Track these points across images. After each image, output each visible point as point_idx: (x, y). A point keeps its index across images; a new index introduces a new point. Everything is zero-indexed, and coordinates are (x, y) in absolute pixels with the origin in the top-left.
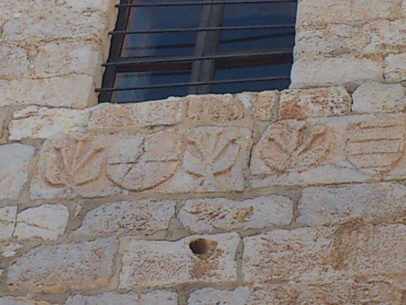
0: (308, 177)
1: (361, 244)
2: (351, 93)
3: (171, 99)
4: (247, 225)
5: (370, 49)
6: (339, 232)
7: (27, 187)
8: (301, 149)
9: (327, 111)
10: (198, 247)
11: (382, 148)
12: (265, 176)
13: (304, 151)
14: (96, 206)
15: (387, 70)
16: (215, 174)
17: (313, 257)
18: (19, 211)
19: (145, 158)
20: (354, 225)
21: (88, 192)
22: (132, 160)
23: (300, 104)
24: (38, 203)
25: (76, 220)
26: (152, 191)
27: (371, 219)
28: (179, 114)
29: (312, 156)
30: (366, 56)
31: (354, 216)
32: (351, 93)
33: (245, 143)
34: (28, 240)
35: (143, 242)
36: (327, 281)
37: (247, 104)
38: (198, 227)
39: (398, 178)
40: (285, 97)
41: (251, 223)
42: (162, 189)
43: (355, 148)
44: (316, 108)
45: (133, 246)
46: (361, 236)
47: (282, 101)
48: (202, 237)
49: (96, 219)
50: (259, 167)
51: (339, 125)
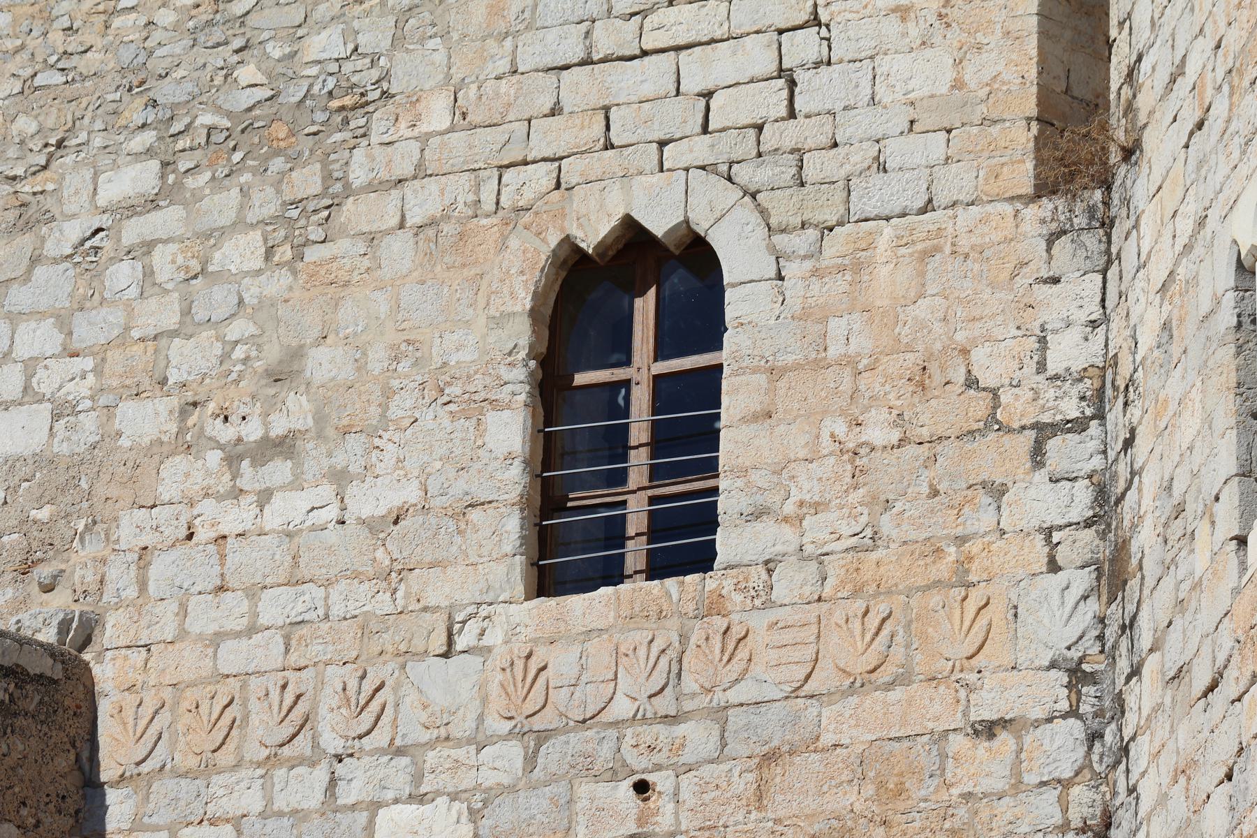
0: (734, 696)
1: (778, 780)
2: (770, 572)
3: (603, 590)
4: (682, 760)
5: (789, 508)
6: (759, 766)
7: (481, 718)
8: (725, 658)
9: (748, 601)
10: (642, 788)
11: (796, 655)
12: (694, 695)
13: (729, 660)
14: (546, 739)
15: (805, 540)
16: (650, 697)
17: (739, 798)
18: (478, 751)
19: (584, 679)
20: (770, 758)
21: (538, 723)
22: (573, 682)
23: (724, 592)
24: (495, 739)
25: (531, 761)
26: (595, 720)
27: (786, 748)
28: (612, 613)
29: (737, 666)
30: (786, 519)
31: (772, 745)
32: (770, 572)
33: (672, 654)
34: (491, 789)
35: (593, 786)
36: (750, 826)
37: (675, 597)
38: (638, 762)
39: (810, 693)
40: (711, 581)
41: (688, 757)
42: (605, 717)
43: (773, 655)
44: (738, 598)
45: (584, 789)
46: (779, 770)
47: (707, 589)
48: (643, 776)
49: (551, 754)
50: (690, 683)
51: (760, 622)
